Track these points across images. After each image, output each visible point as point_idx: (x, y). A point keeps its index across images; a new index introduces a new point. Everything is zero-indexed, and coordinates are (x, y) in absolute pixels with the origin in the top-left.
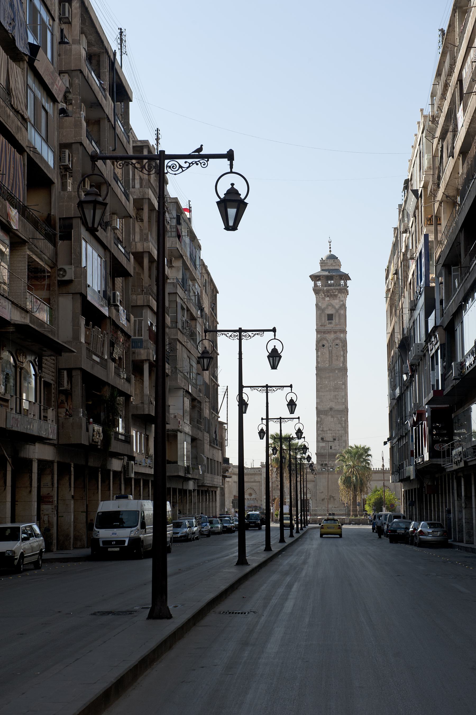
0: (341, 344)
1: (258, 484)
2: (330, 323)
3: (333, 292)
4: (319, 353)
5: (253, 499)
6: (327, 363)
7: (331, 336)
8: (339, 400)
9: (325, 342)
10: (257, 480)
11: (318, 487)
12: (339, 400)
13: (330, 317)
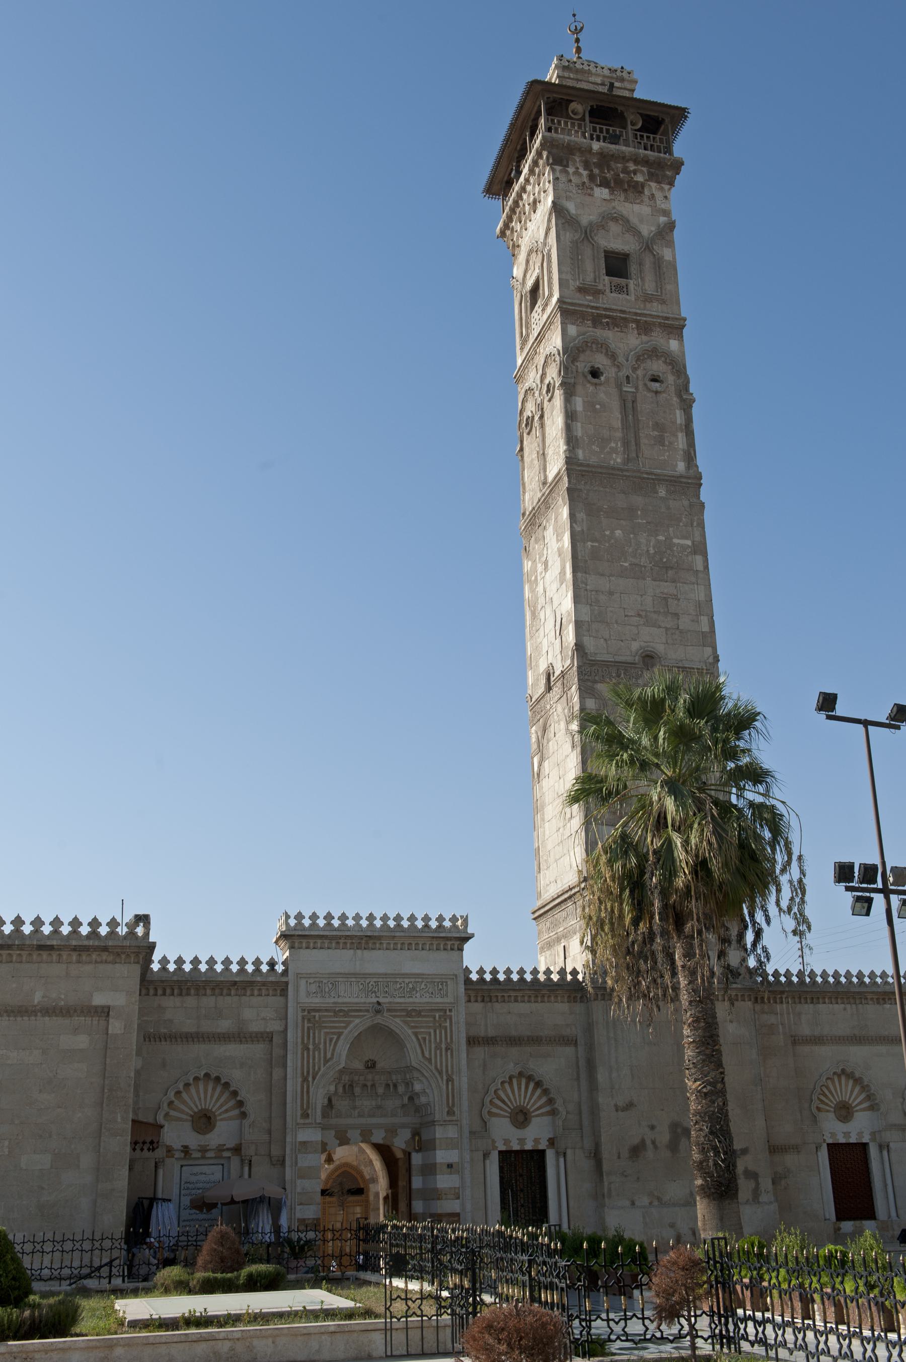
0: (671, 379)
1: (257, 1050)
2: (620, 289)
3: (625, 171)
4: (579, 403)
5: (220, 1149)
6: (614, 450)
7: (629, 342)
8: (685, 622)
9: (601, 361)
10: (255, 1027)
11: (602, 1076)
12: (685, 622)
13: (617, 265)
